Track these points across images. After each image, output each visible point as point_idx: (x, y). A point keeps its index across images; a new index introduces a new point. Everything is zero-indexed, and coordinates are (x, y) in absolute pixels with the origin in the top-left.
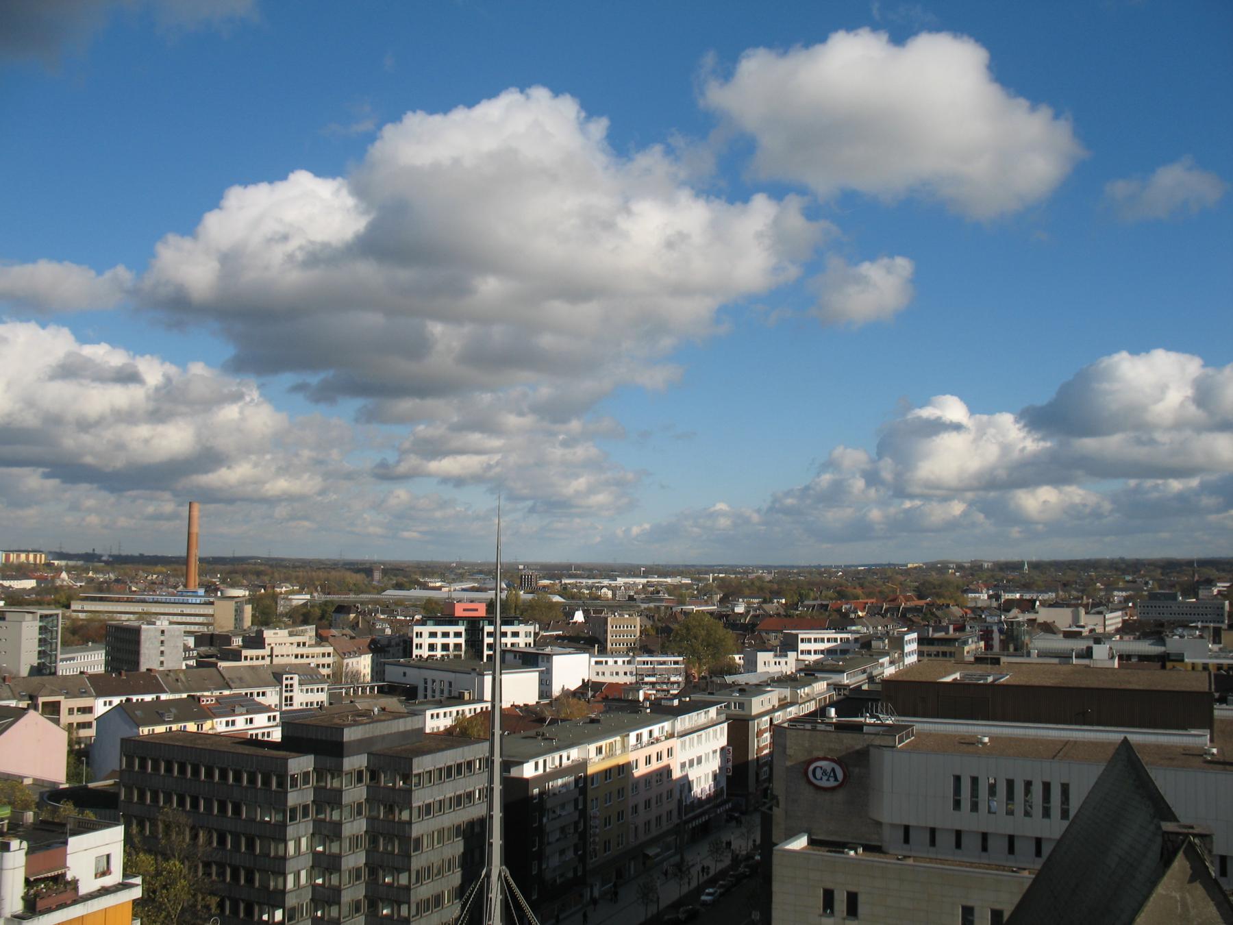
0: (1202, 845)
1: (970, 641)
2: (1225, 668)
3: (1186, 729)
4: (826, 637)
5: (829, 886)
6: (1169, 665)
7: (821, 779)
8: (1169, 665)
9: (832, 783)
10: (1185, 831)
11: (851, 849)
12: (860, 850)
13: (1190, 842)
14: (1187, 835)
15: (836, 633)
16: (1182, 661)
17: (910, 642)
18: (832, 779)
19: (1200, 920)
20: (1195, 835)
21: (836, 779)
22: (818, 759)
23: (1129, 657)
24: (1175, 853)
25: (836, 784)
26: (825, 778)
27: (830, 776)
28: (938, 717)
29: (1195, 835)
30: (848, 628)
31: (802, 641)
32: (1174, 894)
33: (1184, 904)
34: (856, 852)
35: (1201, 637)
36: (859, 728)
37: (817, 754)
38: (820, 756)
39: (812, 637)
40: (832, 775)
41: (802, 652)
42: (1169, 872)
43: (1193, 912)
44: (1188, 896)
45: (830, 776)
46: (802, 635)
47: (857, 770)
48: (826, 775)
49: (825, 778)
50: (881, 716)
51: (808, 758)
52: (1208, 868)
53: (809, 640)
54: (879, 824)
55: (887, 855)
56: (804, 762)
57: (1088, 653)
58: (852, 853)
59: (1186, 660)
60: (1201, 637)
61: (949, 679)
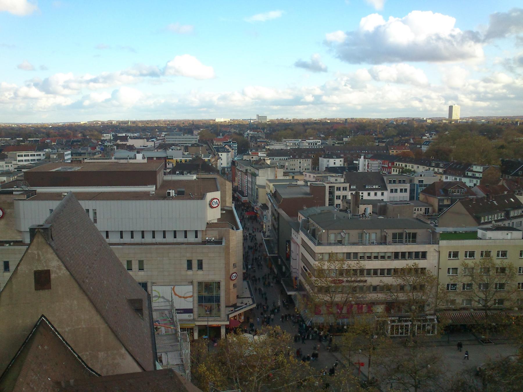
1: (97, 153)
2: (188, 161)
3: (147, 185)
4: (30, 154)
6: (167, 160)
8: (167, 160)
15: (35, 152)
16: (173, 159)
17: (67, 155)
23: (152, 158)
28: (49, 186)
30: (44, 150)
31: (19, 156)
32: (34, 252)
33: (39, 255)
35: (180, 150)
36: (11, 193)
39: (23, 154)
41: (19, 161)
43: (42, 258)
46: (18, 153)
47: (8, 211)
50: (22, 187)
53: (22, 156)
54: (20, 232)
57: (135, 158)
59: (174, 159)
60: (180, 150)
61: (54, 170)
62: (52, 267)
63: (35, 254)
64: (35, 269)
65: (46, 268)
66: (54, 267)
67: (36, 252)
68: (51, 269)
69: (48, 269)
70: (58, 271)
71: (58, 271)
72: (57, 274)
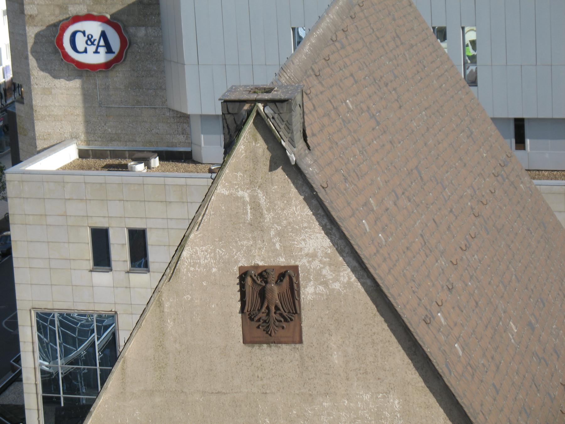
0: (276, 116)
5: (100, 223)
7: (85, 51)
9: (101, 58)
10: (254, 97)
11: (139, 160)
12: (155, 162)
13: (258, 114)
14: (255, 102)
18: (102, 50)
19: (279, 228)
20: (266, 102)
21: (109, 50)
22: (77, 19)
24: (239, 130)
25: (111, 57)
26: (91, 49)
27: (98, 46)
29: (266, 102)
32: (240, 193)
33: (256, 207)
34: (148, 166)
37: (74, 10)
38: (95, 14)
40: (102, 43)
42: (232, 160)
43: (268, 217)
44: (260, 194)
45: (98, 46)
47: (141, 32)
48: (93, 43)
49: (91, 49)
51: (61, 18)
52: (284, 149)
54: (185, 118)
55: (200, 166)
56: (55, 25)
58: (140, 167)
62: (307, 255)
63: (244, 203)
64: (244, 263)
65: (282, 261)
66: (313, 256)
67: (246, 196)
68: (302, 263)
69: (292, 263)
70: (326, 271)
71: (326, 271)
72: (325, 284)
